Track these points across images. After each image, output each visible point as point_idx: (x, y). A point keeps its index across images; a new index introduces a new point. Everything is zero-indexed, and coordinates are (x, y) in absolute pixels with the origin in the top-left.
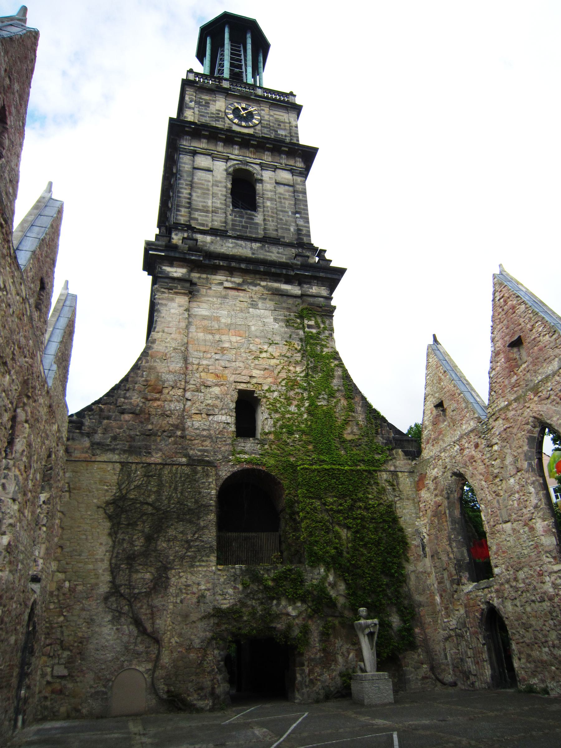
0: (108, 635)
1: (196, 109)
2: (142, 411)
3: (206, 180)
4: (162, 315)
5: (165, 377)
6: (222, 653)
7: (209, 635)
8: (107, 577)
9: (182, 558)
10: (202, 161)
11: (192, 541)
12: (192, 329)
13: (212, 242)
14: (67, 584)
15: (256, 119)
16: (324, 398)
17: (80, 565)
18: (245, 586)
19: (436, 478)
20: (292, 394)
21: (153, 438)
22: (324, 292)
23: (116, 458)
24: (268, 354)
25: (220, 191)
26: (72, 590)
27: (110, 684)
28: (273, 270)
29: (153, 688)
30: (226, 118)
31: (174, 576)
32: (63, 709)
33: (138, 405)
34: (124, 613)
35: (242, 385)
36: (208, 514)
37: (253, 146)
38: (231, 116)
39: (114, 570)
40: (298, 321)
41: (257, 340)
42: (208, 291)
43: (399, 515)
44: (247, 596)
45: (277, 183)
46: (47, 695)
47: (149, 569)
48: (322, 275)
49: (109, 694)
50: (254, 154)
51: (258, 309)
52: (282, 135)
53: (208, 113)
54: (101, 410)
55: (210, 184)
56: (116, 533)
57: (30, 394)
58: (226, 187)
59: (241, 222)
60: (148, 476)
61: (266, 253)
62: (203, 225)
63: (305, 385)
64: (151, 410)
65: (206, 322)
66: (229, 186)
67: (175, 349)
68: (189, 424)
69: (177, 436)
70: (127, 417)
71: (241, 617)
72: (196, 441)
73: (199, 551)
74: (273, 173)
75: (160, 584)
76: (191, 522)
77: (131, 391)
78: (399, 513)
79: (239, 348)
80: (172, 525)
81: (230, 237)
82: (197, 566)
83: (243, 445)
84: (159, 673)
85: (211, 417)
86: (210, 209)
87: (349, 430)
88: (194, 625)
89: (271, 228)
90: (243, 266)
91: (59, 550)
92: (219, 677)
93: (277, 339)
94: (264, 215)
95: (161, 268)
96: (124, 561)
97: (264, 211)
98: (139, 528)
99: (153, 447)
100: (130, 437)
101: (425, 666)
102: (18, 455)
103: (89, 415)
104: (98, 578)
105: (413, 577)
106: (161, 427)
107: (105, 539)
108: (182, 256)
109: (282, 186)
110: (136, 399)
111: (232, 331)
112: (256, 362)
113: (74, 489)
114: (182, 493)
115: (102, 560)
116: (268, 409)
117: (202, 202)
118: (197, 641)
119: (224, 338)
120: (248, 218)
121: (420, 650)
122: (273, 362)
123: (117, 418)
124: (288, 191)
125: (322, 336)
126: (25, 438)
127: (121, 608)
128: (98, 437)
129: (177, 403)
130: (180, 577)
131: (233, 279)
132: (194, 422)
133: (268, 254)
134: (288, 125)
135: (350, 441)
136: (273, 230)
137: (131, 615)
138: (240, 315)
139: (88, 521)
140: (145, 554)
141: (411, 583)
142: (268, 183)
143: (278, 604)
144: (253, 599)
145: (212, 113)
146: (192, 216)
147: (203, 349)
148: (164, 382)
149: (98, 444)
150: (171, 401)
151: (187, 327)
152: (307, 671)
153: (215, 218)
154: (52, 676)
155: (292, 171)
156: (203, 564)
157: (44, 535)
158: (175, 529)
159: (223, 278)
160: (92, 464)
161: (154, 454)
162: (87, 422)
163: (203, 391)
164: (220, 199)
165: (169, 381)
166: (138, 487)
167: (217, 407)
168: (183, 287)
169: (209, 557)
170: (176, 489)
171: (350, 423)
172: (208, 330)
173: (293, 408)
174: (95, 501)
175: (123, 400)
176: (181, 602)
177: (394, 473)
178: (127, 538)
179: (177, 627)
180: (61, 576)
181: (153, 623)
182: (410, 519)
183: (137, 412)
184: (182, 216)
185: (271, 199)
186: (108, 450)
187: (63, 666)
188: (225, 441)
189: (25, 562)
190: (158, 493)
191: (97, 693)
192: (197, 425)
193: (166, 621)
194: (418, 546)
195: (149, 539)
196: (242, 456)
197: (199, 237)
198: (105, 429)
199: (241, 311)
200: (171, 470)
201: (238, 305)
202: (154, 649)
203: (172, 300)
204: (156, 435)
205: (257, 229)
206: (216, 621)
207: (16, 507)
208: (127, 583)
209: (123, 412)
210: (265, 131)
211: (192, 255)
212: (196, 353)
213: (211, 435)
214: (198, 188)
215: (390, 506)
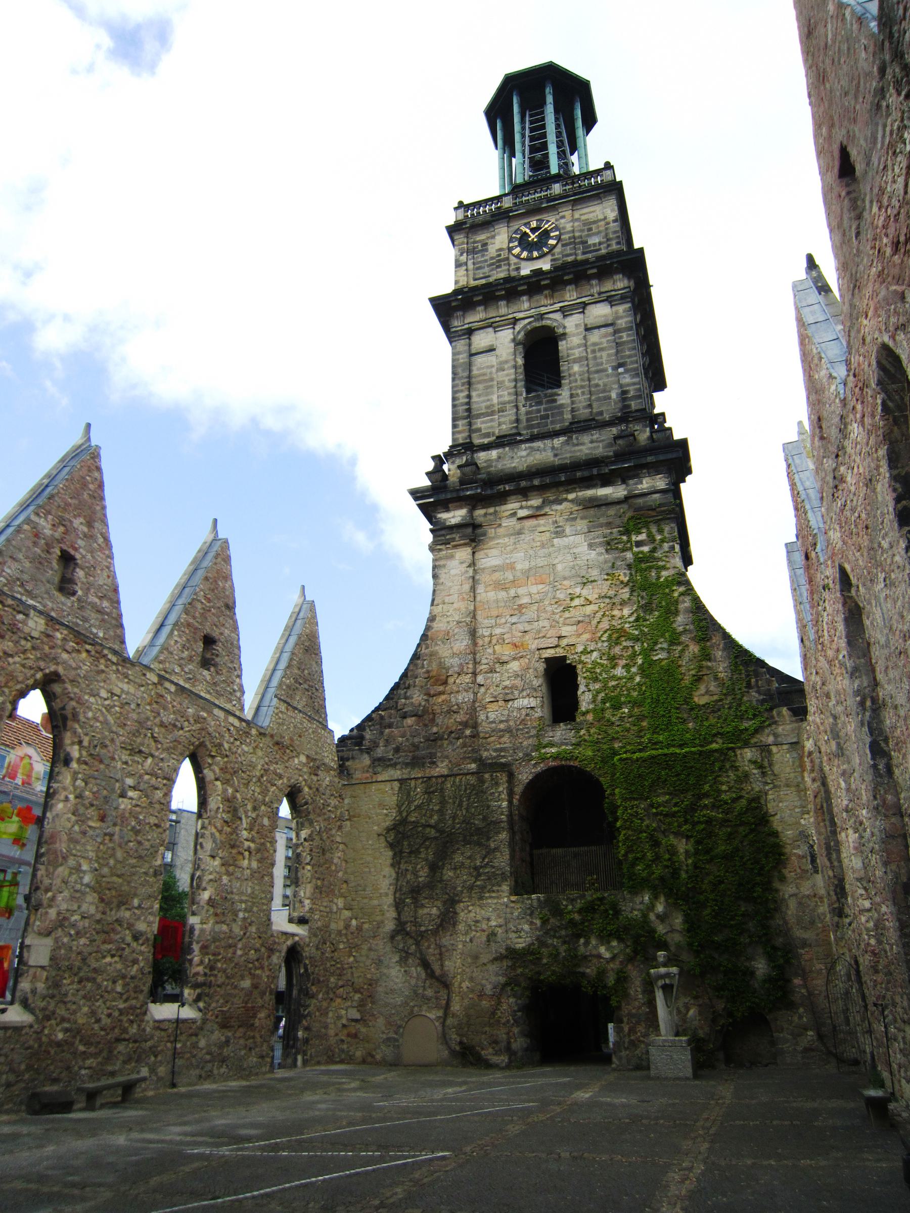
0: (397, 978)
1: (470, 263)
2: (425, 711)
3: (488, 367)
4: (441, 581)
5: (449, 662)
6: (519, 1002)
7: (502, 980)
8: (392, 914)
9: (471, 888)
10: (481, 340)
11: (481, 867)
12: (480, 589)
13: (499, 457)
14: (354, 922)
15: (552, 238)
16: (662, 649)
17: (366, 901)
18: (545, 922)
19: (810, 753)
20: (617, 650)
21: (439, 743)
22: (661, 482)
23: (397, 774)
24: (582, 599)
25: (507, 375)
26: (359, 928)
27: (401, 1030)
28: (579, 474)
29: (444, 1038)
30: (511, 257)
31: (463, 911)
32: (358, 1054)
33: (420, 705)
34: (411, 954)
35: (549, 651)
36: (499, 833)
37: (546, 287)
38: (517, 251)
39: (398, 905)
40: (625, 538)
41: (565, 582)
42: (498, 530)
43: (771, 811)
44: (546, 933)
45: (588, 329)
46: (343, 1038)
47: (435, 903)
48: (650, 459)
49: (401, 1040)
50: (552, 297)
51: (565, 536)
52: (594, 245)
53: (486, 261)
54: (382, 717)
55: (494, 370)
56: (399, 863)
57: (213, 754)
58: (515, 367)
59: (539, 411)
60: (430, 793)
61: (573, 449)
62: (487, 435)
63: (637, 633)
64: (435, 707)
65: (497, 576)
66: (520, 361)
67: (458, 622)
68: (482, 717)
69: (466, 737)
70: (410, 721)
71: (540, 959)
72: (492, 739)
73: (489, 879)
74: (581, 316)
75: (448, 920)
76: (479, 844)
77: (412, 688)
78: (771, 807)
79: (541, 601)
80: (458, 849)
81: (521, 442)
82: (487, 898)
83: (551, 734)
84: (449, 1021)
85: (510, 703)
87: (702, 688)
88: (485, 967)
89: (581, 405)
90: (536, 482)
91: (345, 886)
92: (516, 1030)
93: (594, 573)
94: (571, 389)
95: (436, 518)
96: (409, 895)
97: (570, 383)
98: (423, 856)
99: (439, 754)
100: (413, 745)
101: (810, 1033)
102: (212, 813)
103: (370, 726)
104: (383, 914)
105: (792, 904)
106: (447, 727)
107: (388, 871)
108: (454, 495)
109: (596, 331)
110: (417, 697)
111: (532, 579)
112: (567, 615)
113: (354, 817)
114: (467, 809)
115: (387, 895)
116: (585, 678)
117: (484, 401)
118: (489, 987)
119: (521, 591)
120: (548, 402)
121: (801, 1010)
122: (589, 609)
123: (399, 724)
124: (605, 336)
125: (658, 554)
126: (218, 795)
127: (408, 948)
128: (380, 751)
129: (465, 694)
130: (470, 911)
131: (530, 503)
132: (490, 714)
133: (577, 448)
134: (603, 223)
135: (703, 706)
136: (585, 408)
137: (418, 955)
138: (542, 552)
139: (370, 852)
140: (430, 886)
141: (790, 913)
142: (574, 335)
143: (587, 943)
144: (554, 937)
145: (492, 258)
146: (474, 427)
147: (495, 613)
148: (448, 669)
149: (379, 759)
150: (458, 692)
151: (473, 589)
152: (626, 1029)
153: (502, 420)
154: (348, 1020)
155: (610, 300)
156: (494, 895)
157: (309, 875)
158: (462, 854)
159: (517, 505)
160: (370, 785)
161: (439, 764)
162: (368, 735)
163: (498, 670)
164: (507, 388)
165: (452, 666)
166: (418, 807)
167: (516, 688)
168: (461, 538)
169: (500, 886)
170: (460, 805)
171: (705, 677)
172: (501, 586)
173: (619, 671)
174: (375, 828)
175: (403, 701)
176: (471, 941)
177: (765, 749)
178: (410, 868)
179: (467, 970)
180: (347, 913)
181: (442, 965)
182: (791, 816)
183: (420, 713)
184: (459, 432)
185: (578, 360)
186: (388, 766)
187: (355, 1010)
188: (527, 733)
189: (255, 909)
190: (441, 812)
191: (388, 1039)
192: (492, 716)
193: (455, 963)
194: (803, 857)
195: (434, 868)
196: (548, 750)
197: (482, 457)
198: (387, 740)
199: (543, 546)
200: (454, 782)
201: (538, 539)
202: (443, 994)
203: (452, 557)
204: (442, 739)
205: (562, 413)
206: (510, 964)
207: (217, 862)
208: (412, 919)
209: (404, 717)
210: (568, 250)
211: (467, 489)
212: (486, 621)
213: (509, 727)
214: (479, 382)
215: (756, 799)
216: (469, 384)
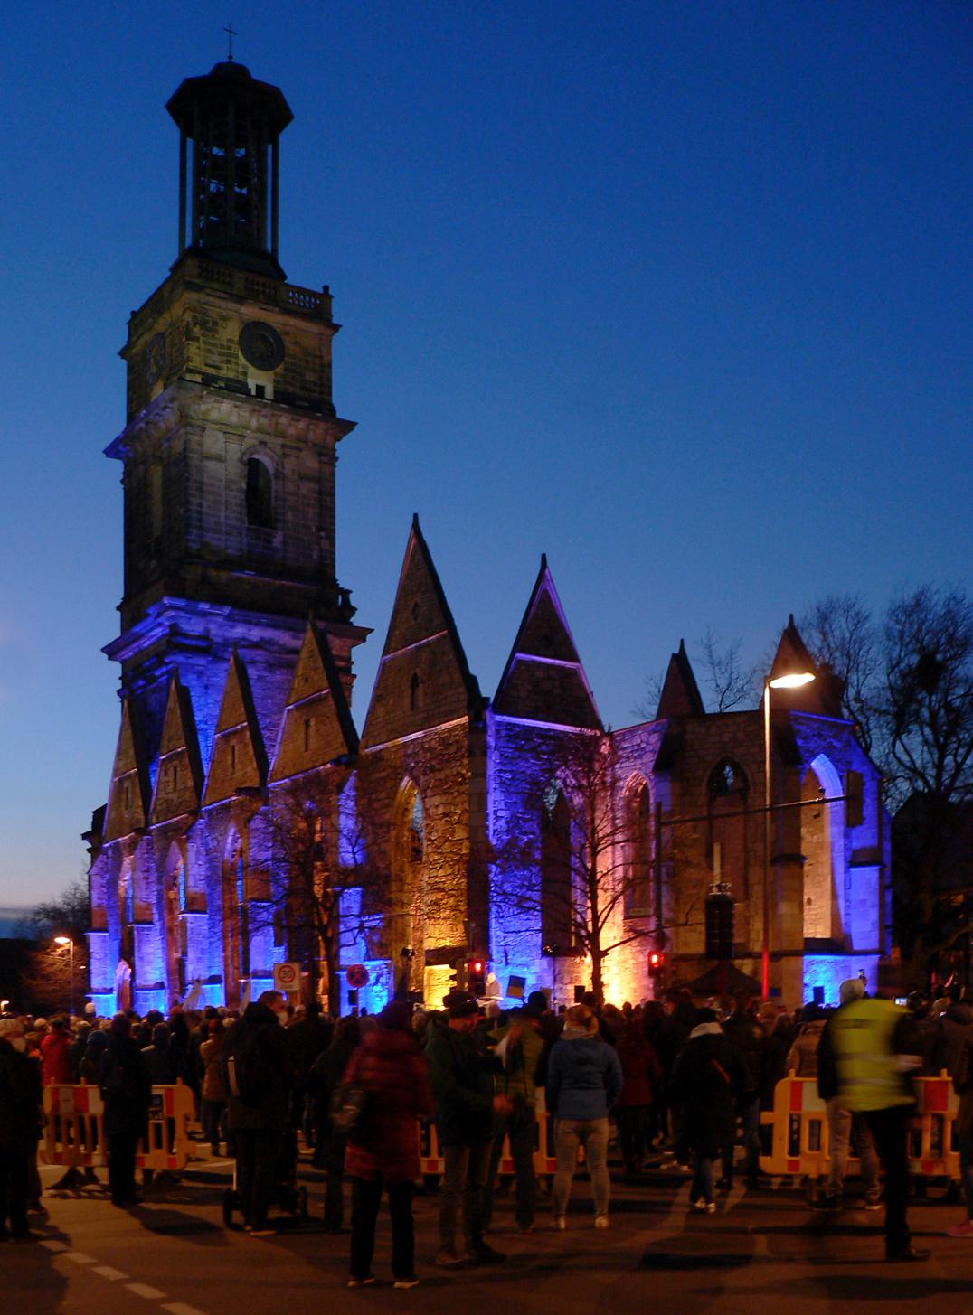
53: (215, 345)
55: (223, 484)
58: (240, 490)
66: (244, 485)
86: (224, 528)
94: (284, 536)
134: (318, 361)
145: (222, 346)
153: (229, 544)
216: (200, 489)
